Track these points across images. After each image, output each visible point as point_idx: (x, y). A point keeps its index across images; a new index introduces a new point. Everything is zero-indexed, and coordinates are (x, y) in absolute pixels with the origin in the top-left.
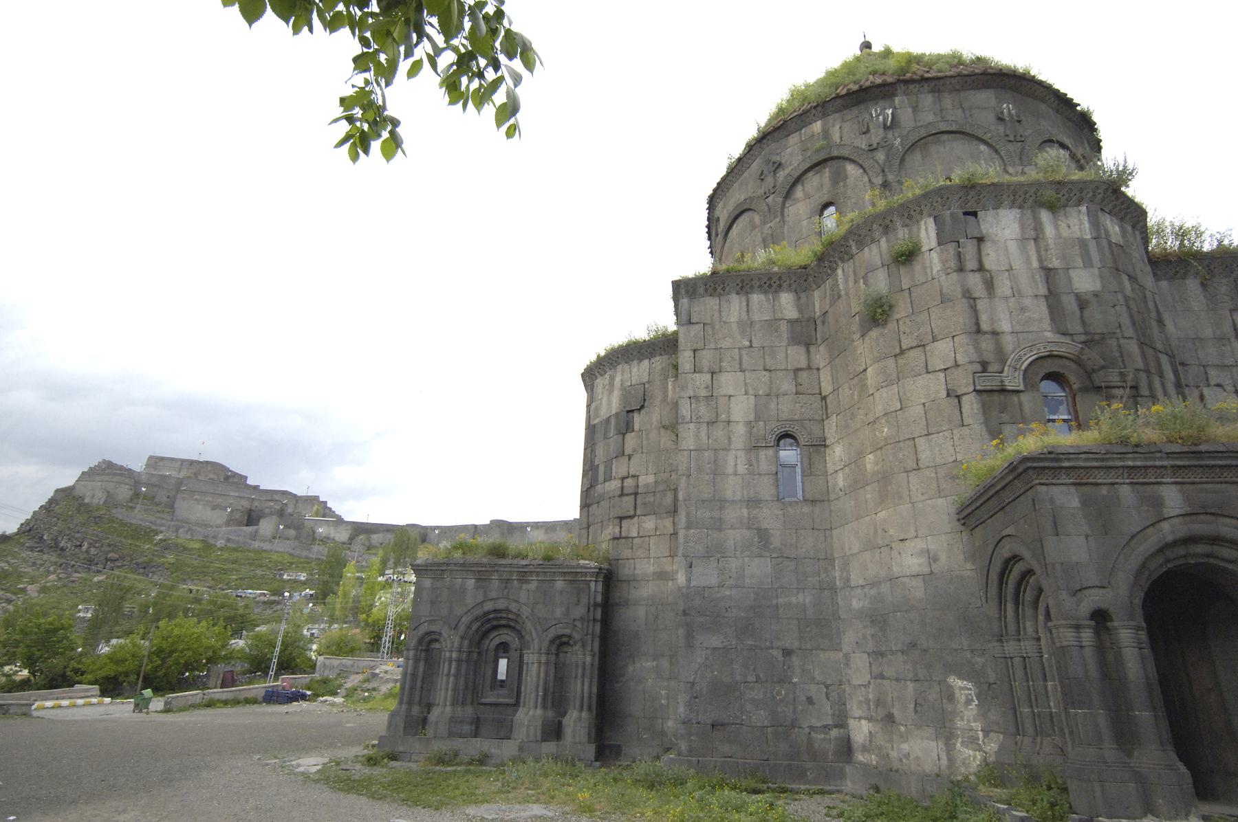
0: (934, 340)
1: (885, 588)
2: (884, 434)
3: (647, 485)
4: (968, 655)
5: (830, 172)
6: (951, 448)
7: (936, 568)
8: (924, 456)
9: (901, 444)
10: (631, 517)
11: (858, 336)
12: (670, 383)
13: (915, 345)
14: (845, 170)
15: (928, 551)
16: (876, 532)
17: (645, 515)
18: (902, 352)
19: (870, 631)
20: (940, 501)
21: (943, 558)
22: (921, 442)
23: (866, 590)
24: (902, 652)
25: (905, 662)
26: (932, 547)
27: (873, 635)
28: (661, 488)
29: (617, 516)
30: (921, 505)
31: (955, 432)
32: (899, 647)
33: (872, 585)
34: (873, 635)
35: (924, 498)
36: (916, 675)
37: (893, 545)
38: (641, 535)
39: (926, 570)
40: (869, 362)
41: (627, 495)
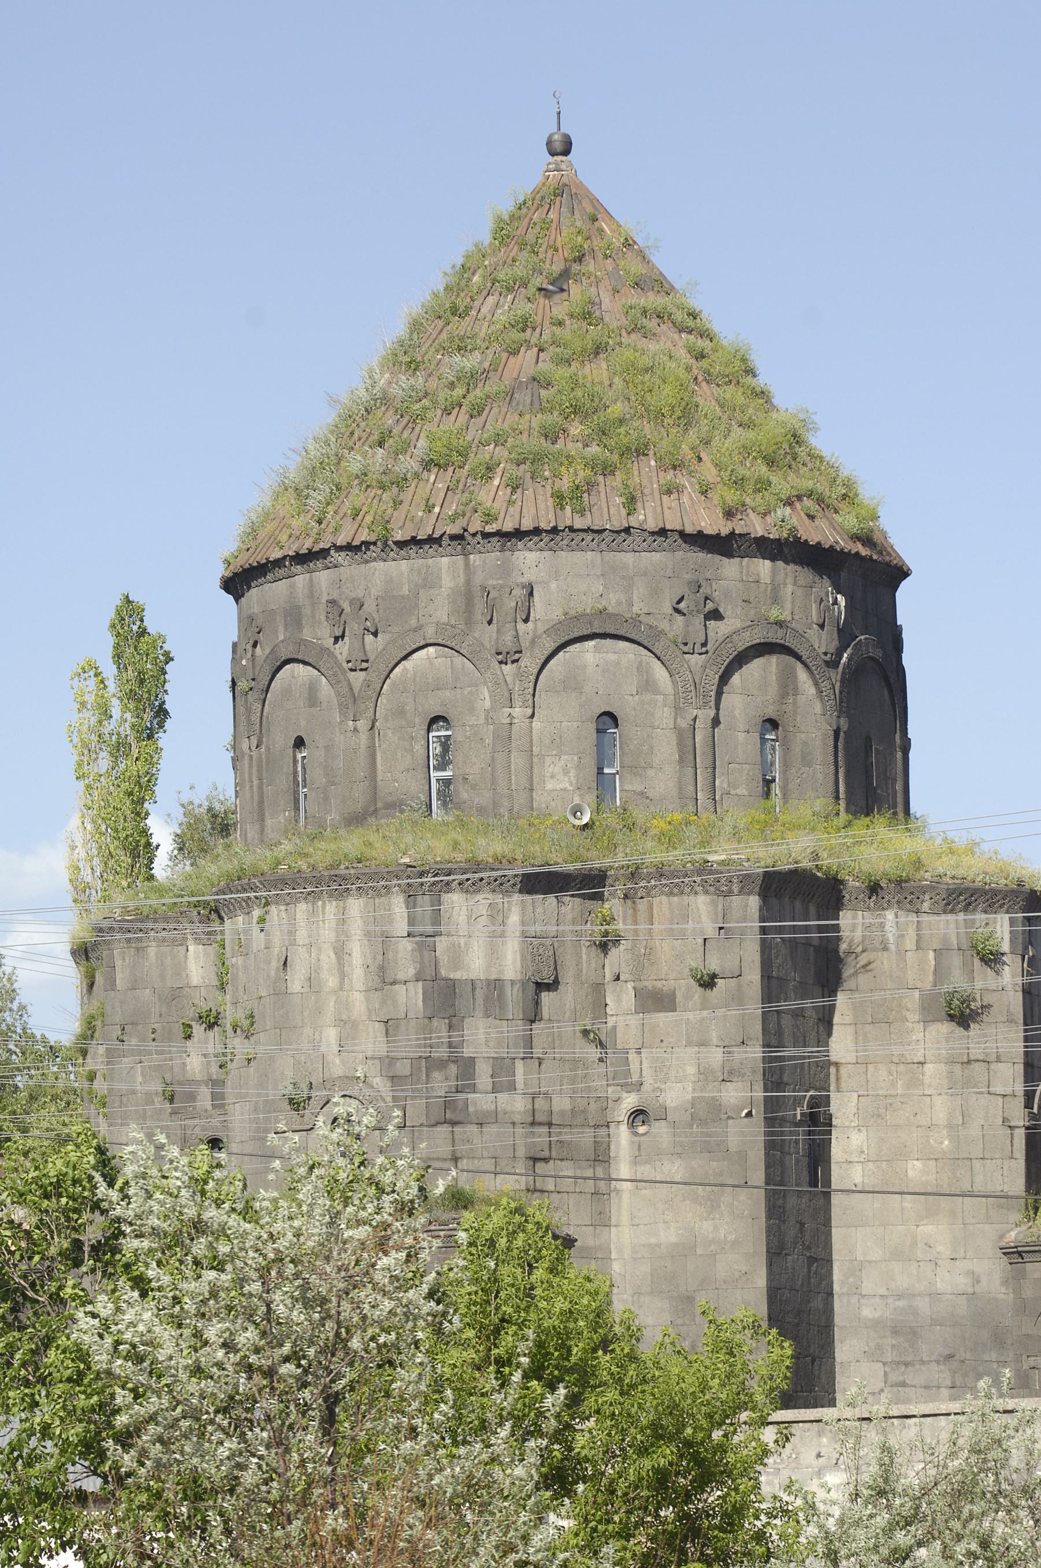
0: (999, 1060)
1: (923, 1305)
2: (944, 1146)
3: (562, 1113)
4: (995, 1366)
5: (778, 664)
6: (1000, 1177)
7: (978, 1289)
8: (979, 1179)
9: (960, 1162)
10: (546, 1160)
11: (917, 1017)
12: (584, 949)
13: (981, 1058)
14: (796, 677)
15: (973, 1273)
16: (915, 1243)
17: (562, 1160)
18: (969, 1062)
19: (889, 1341)
20: (987, 1227)
21: (984, 1280)
22: (977, 1164)
23: (890, 1300)
24: (938, 1362)
25: (941, 1371)
26: (977, 1269)
27: (893, 1346)
28: (579, 1120)
29: (531, 1155)
30: (971, 1228)
31: (1005, 1162)
32: (934, 1358)
33: (900, 1297)
34: (893, 1346)
35: (973, 1221)
36: (953, 1382)
37: (940, 1262)
38: (558, 1189)
39: (970, 1290)
40: (929, 1057)
41: (540, 1124)
